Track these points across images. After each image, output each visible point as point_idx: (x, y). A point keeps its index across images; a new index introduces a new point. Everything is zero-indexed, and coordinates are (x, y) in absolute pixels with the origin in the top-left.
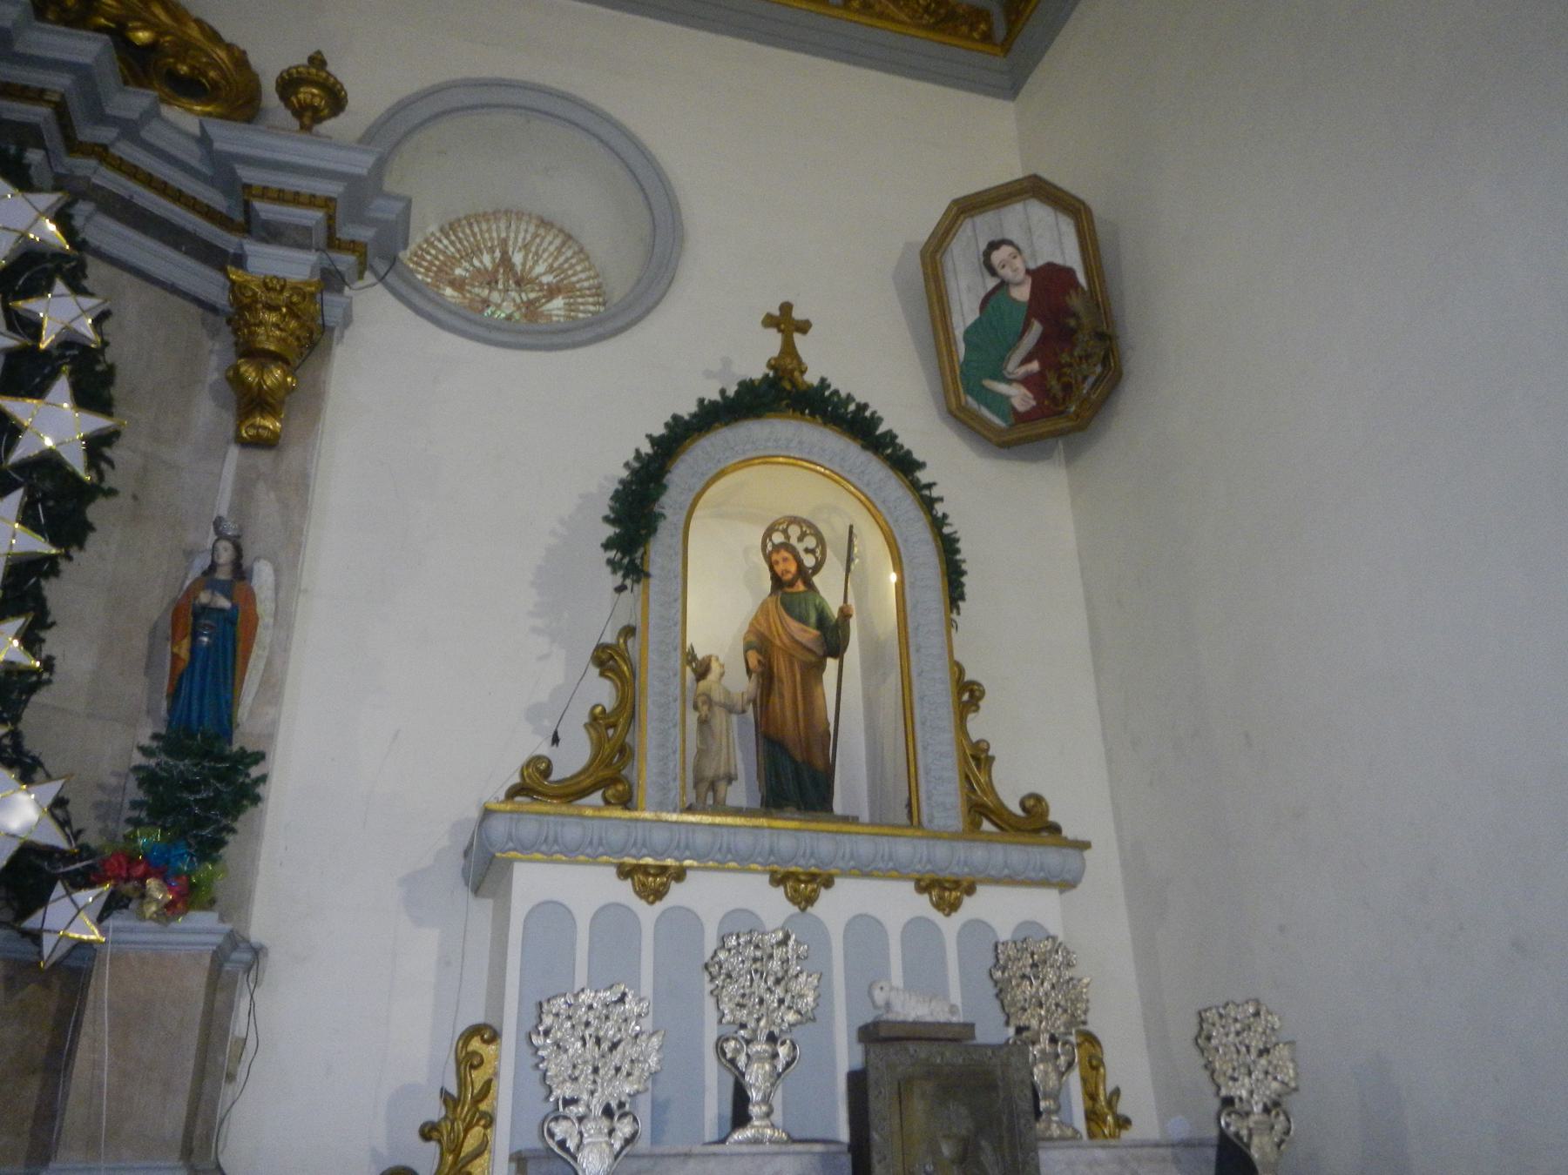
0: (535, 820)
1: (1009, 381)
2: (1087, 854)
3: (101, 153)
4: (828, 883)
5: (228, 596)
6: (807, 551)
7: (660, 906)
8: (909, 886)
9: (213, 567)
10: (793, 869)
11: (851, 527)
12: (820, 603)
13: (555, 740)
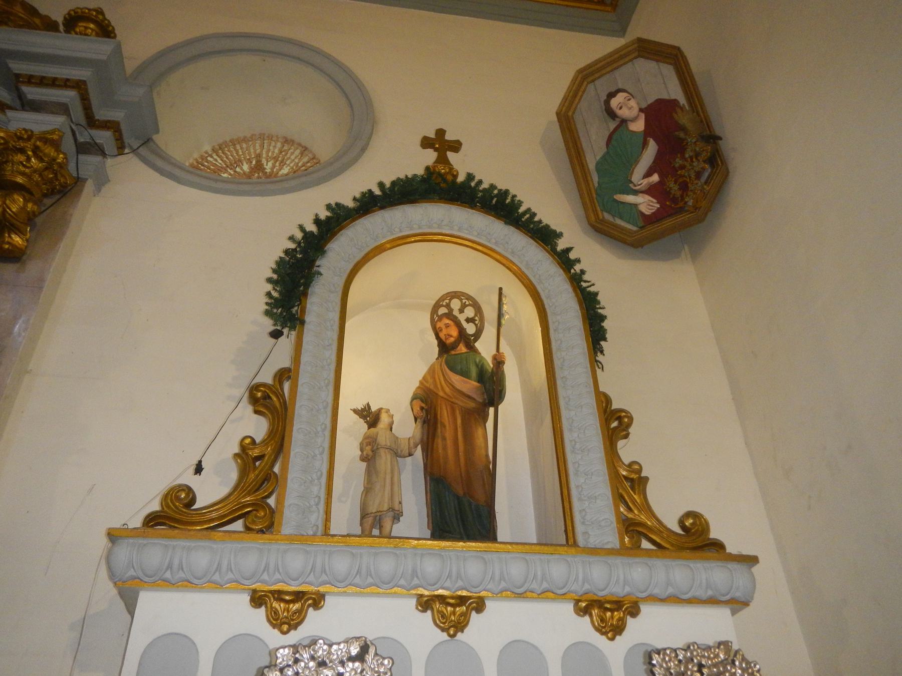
1: (636, 193)
2: (756, 569)
6: (468, 320)
10: (441, 592)
11: (501, 289)
12: (480, 362)
13: (199, 469)
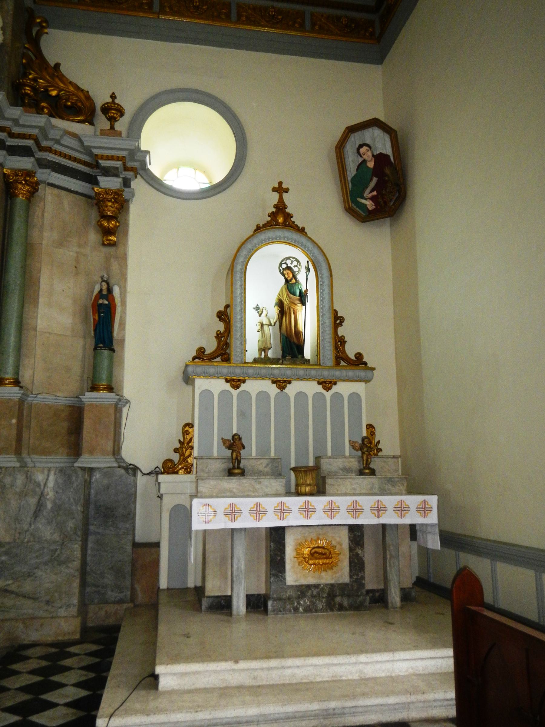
0: (201, 367)
1: (366, 199)
2: (374, 372)
3: (49, 150)
4: (290, 383)
5: (107, 300)
7: (238, 390)
8: (315, 383)
9: (101, 290)
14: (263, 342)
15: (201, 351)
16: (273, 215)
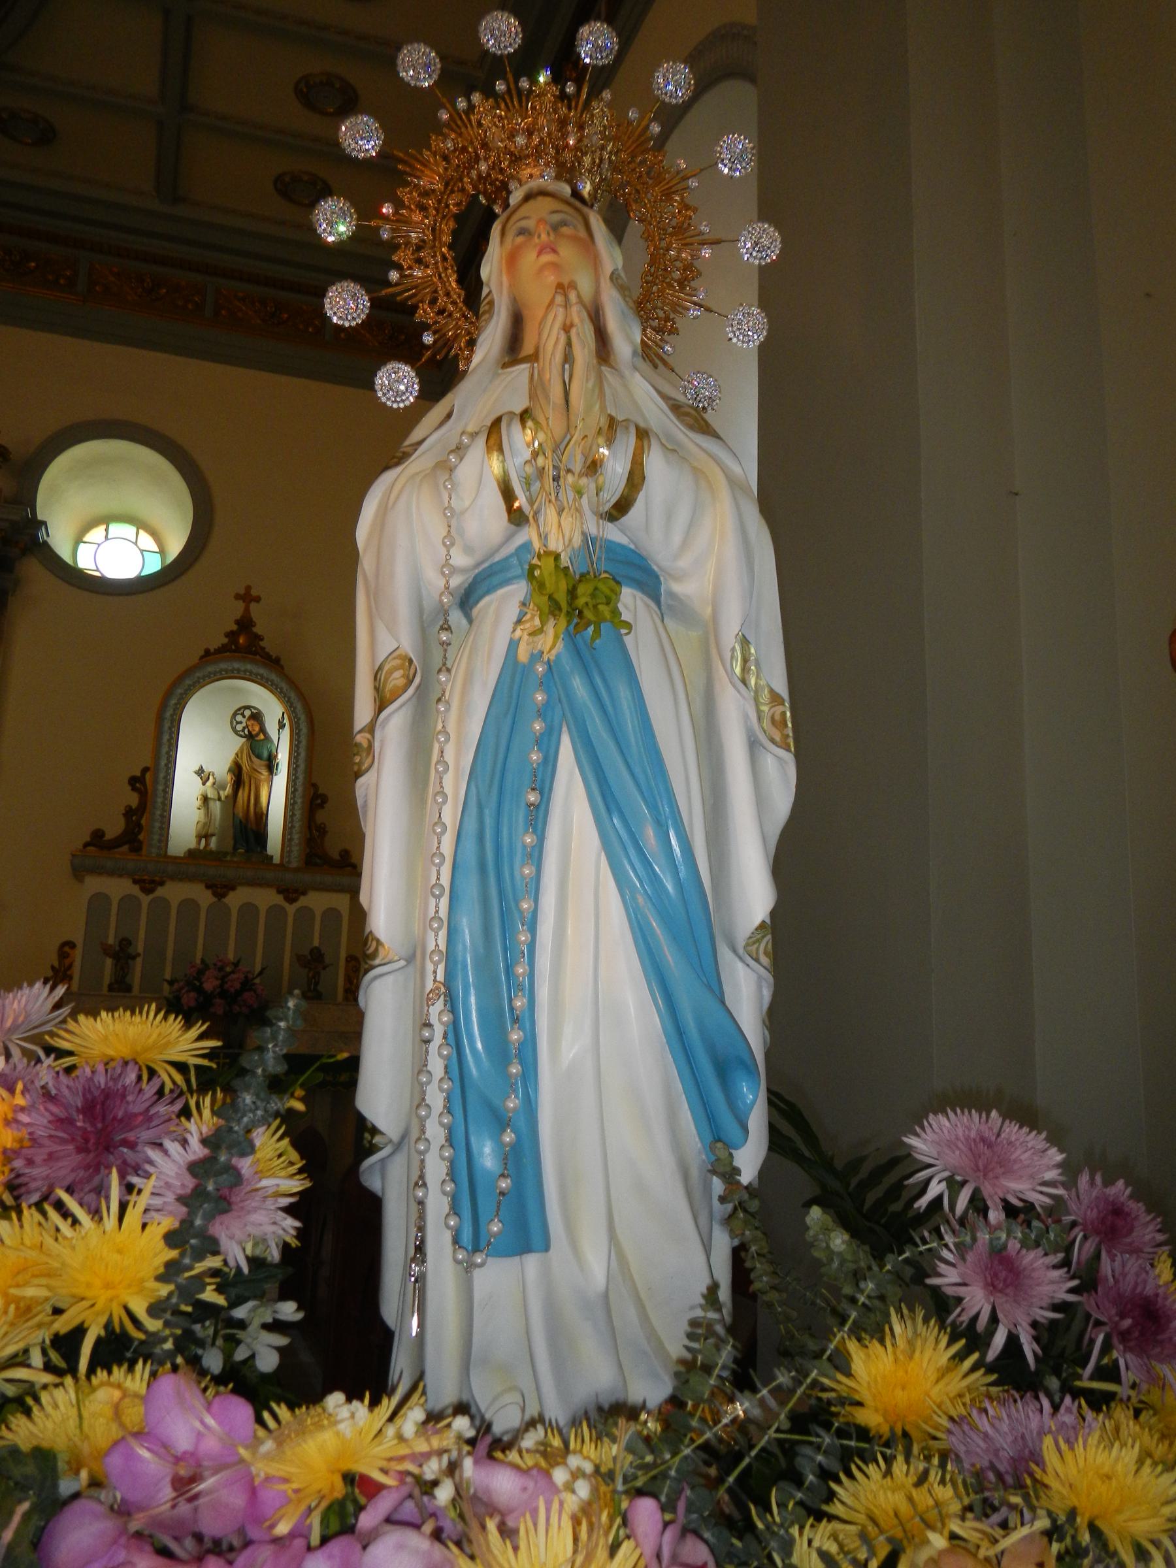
4: (233, 888)
7: (151, 896)
14: (205, 824)
15: (98, 835)
16: (231, 635)
